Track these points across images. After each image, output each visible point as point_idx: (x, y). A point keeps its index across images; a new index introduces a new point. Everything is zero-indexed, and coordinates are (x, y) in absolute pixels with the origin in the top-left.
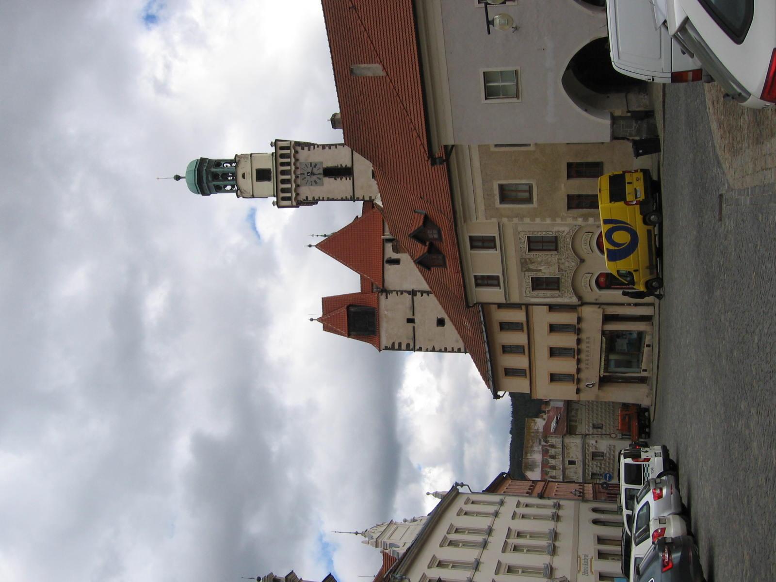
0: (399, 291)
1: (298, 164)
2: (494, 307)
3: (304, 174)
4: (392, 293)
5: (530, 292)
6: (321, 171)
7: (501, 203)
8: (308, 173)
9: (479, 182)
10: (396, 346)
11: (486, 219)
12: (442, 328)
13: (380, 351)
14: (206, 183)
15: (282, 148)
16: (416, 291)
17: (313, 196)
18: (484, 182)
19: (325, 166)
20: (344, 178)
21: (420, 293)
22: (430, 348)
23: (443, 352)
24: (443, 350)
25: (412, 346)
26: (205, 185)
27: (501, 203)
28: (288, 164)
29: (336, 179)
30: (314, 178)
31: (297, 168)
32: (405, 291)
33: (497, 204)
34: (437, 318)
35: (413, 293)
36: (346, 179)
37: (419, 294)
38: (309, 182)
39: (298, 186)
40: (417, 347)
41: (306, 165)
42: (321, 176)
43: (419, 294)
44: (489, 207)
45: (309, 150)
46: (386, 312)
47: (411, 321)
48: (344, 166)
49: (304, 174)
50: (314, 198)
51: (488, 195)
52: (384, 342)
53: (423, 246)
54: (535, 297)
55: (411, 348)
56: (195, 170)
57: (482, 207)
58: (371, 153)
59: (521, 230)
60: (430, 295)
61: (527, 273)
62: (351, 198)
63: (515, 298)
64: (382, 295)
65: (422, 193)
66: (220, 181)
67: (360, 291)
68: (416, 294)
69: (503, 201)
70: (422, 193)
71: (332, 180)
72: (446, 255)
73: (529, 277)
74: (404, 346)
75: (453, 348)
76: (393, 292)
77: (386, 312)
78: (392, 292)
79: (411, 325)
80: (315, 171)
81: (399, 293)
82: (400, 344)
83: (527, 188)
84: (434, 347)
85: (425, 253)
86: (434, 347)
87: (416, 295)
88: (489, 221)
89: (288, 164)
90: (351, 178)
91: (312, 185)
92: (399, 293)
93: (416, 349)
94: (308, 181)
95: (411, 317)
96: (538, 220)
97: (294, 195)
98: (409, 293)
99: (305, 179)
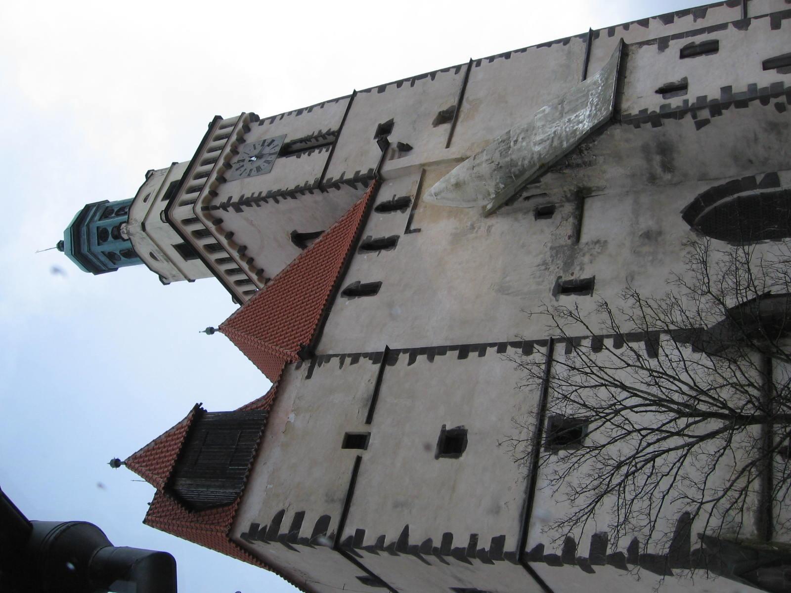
0: (349, 355)
1: (241, 149)
3: (243, 161)
4: (328, 361)
6: (278, 149)
12: (453, 460)
14: (88, 225)
16: (398, 352)
19: (287, 140)
20: (317, 151)
21: (407, 355)
22: (392, 537)
24: (437, 543)
25: (333, 527)
26: (84, 229)
30: (261, 163)
31: (235, 151)
32: (366, 355)
34: (444, 426)
35: (387, 358)
36: (320, 152)
37: (404, 358)
38: (248, 171)
39: (222, 180)
41: (254, 145)
43: (404, 358)
46: (292, 416)
48: (324, 131)
49: (243, 161)
52: (256, 509)
60: (437, 358)
64: (298, 368)
68: (396, 360)
71: (293, 159)
75: (474, 538)
77: (292, 416)
79: (354, 452)
81: (348, 360)
82: (299, 517)
84: (407, 528)
86: (407, 528)
91: (249, 175)
92: (348, 360)
93: (344, 537)
94: (245, 169)
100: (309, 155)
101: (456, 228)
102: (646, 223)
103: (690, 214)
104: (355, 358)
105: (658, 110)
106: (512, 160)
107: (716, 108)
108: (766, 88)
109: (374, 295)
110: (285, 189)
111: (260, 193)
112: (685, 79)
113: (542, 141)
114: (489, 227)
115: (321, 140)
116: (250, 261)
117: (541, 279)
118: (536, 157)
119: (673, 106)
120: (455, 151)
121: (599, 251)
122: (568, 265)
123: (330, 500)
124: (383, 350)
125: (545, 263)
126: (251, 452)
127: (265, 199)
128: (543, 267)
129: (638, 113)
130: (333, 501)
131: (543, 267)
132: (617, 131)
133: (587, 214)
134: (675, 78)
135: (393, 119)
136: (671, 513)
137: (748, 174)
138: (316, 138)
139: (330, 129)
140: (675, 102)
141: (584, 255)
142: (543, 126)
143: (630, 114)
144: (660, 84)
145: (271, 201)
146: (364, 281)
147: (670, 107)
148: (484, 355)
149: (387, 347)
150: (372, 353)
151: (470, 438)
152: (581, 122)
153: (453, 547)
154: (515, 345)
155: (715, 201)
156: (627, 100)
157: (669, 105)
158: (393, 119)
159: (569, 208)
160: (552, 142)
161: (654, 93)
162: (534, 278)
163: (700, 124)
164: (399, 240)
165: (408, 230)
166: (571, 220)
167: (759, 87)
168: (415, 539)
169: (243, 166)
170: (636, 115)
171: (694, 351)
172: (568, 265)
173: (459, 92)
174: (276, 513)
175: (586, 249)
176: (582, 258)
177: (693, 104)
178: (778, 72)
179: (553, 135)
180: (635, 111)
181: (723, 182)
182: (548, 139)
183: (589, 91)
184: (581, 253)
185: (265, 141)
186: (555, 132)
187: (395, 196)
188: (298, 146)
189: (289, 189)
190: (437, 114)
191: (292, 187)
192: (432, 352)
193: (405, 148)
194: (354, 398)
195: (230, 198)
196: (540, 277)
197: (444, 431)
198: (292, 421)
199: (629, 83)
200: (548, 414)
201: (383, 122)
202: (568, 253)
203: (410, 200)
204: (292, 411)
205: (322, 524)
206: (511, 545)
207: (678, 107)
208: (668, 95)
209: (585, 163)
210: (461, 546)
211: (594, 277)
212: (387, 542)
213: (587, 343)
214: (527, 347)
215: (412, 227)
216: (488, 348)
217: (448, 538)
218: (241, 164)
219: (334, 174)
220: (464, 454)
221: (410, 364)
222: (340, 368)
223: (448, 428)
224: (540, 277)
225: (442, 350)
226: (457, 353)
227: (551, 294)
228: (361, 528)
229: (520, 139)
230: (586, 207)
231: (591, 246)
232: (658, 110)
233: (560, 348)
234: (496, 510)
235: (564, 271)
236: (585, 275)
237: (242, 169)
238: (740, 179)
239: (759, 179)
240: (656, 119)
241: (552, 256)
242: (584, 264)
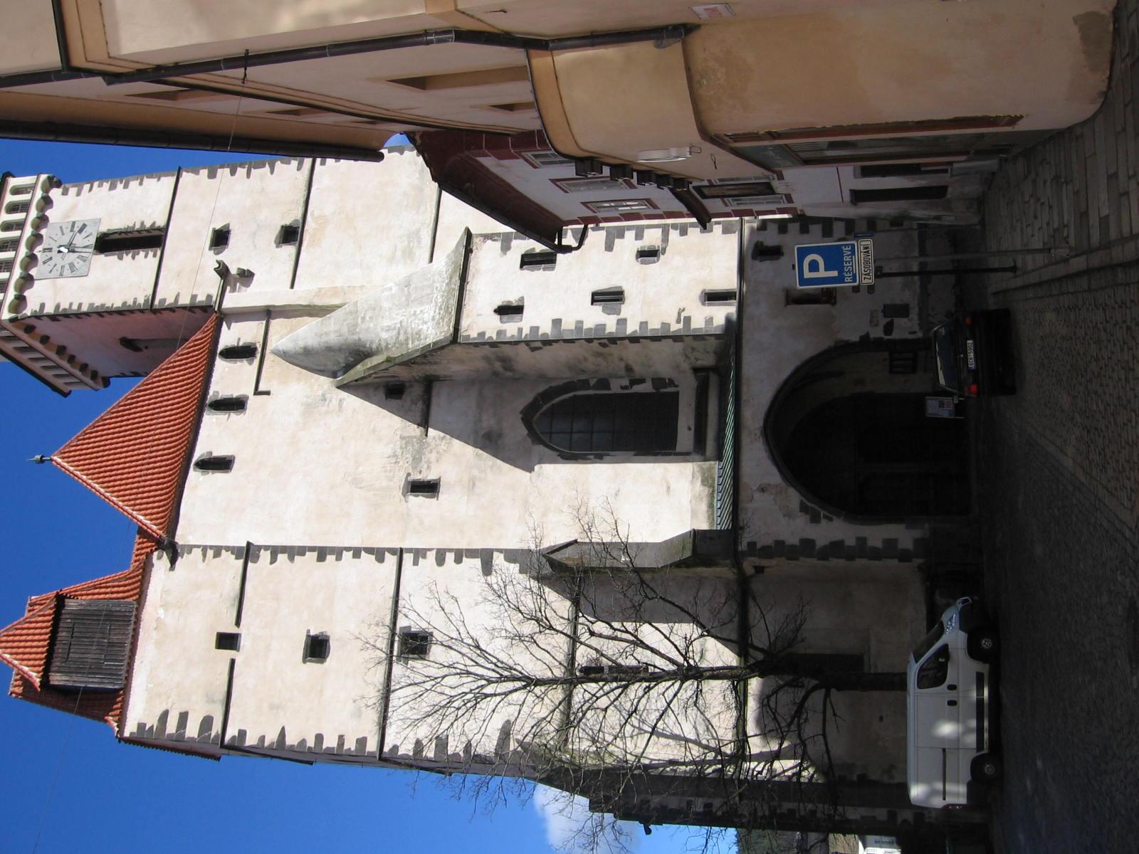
0: (211, 547)
3: (50, 250)
4: (190, 552)
6: (92, 241)
8: (61, 246)
16: (259, 548)
17: (57, 302)
19: (104, 229)
20: (142, 253)
24: (311, 743)
25: (217, 728)
29: (121, 258)
31: (37, 238)
32: (228, 549)
34: (308, 631)
35: (248, 553)
36: (146, 256)
37: (265, 556)
38: (59, 267)
41: (61, 227)
43: (265, 556)
46: (161, 612)
47: (227, 641)
48: (148, 225)
49: (50, 250)
55: (213, 733)
60: (297, 558)
62: (146, 301)
64: (160, 558)
68: (258, 557)
75: (341, 738)
76: (194, 550)
78: (190, 548)
79: (229, 654)
80: (80, 241)
81: (210, 553)
82: (184, 717)
84: (283, 729)
86: (283, 729)
90: (159, 253)
91: (61, 275)
92: (210, 553)
93: (228, 738)
95: (232, 629)
99: (49, 263)
100: (133, 258)
101: (307, 397)
102: (488, 422)
103: (528, 416)
104: (218, 551)
105: (495, 337)
106: (360, 339)
107: (547, 342)
108: (590, 329)
109: (227, 472)
110: (110, 305)
111: (80, 305)
112: (522, 299)
113: (388, 329)
114: (340, 401)
115: (145, 234)
116: (72, 359)
117: (392, 474)
118: (383, 344)
119: (509, 334)
120: (299, 296)
121: (445, 448)
122: (417, 460)
123: (210, 700)
124: (244, 545)
125: (395, 455)
126: (125, 647)
127: (87, 314)
128: (394, 460)
129: (475, 335)
130: (213, 701)
131: (393, 460)
132: (458, 349)
133: (434, 401)
134: (513, 299)
135: (229, 224)
136: (497, 723)
137: (583, 377)
138: (139, 231)
139: (154, 223)
140: (511, 328)
141: (431, 451)
142: (390, 309)
143: (469, 336)
144: (498, 302)
145: (95, 316)
146: (217, 453)
147: (505, 335)
148: (341, 560)
149: (249, 544)
150: (234, 547)
151: (333, 645)
152: (426, 323)
153: (324, 747)
154: (370, 551)
155: (552, 399)
156: (468, 316)
157: (505, 331)
158: (229, 224)
159: (417, 391)
160: (399, 334)
161: (493, 313)
162: (385, 471)
163: (533, 349)
164: (249, 402)
165: (257, 392)
166: (420, 404)
167: (586, 326)
168: (291, 740)
169: (51, 259)
170: (475, 339)
171: (521, 572)
172: (417, 460)
173: (303, 200)
174: (161, 712)
175: (433, 445)
176: (429, 455)
177: (526, 335)
178: (603, 311)
179: (399, 325)
180: (474, 334)
181: (561, 383)
182: (394, 329)
183: (434, 282)
184: (429, 449)
185: (74, 223)
186: (401, 322)
187: (239, 339)
188: (116, 236)
189: (115, 306)
190: (279, 228)
191: (118, 304)
192: (294, 552)
193: (246, 276)
194: (221, 596)
195: (43, 306)
196: (390, 471)
197: (308, 636)
198: (162, 617)
199: (470, 291)
200: (398, 627)
201: (218, 227)
202: (417, 446)
203: (256, 349)
204: (161, 606)
205: (207, 722)
206: (372, 746)
207: (513, 336)
208: (505, 317)
209: (430, 362)
210: (331, 745)
211: (440, 479)
212: (267, 744)
213: (431, 556)
214: (379, 554)
215: (261, 388)
216: (344, 552)
218: (49, 254)
219: (167, 294)
220: (328, 659)
221: (272, 563)
222: (204, 561)
223: (312, 633)
224: (390, 471)
225: (302, 551)
226: (315, 554)
227: (400, 493)
228: (243, 728)
229: (367, 318)
230: (434, 392)
231: (438, 442)
232: (495, 337)
233: (408, 558)
234: (358, 714)
235: (413, 468)
236: (430, 476)
237: (52, 263)
238: (575, 380)
239: (592, 382)
240: (493, 345)
241: (401, 448)
242: (431, 463)
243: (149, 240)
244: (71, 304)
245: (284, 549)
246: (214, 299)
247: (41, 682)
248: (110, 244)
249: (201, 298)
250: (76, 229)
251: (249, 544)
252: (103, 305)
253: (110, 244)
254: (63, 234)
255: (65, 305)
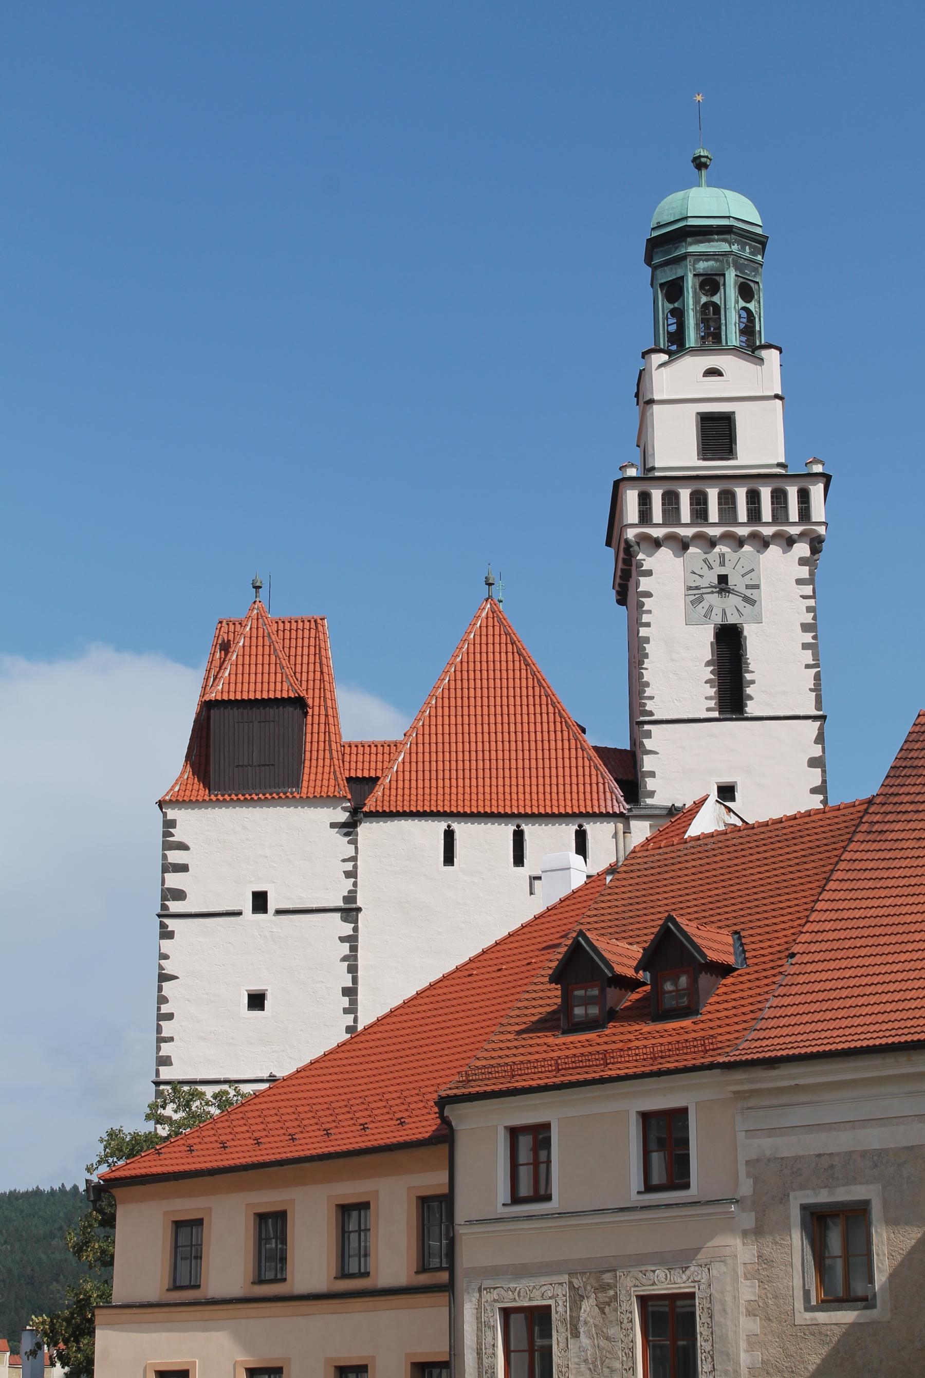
0: (355, 867)
2: (433, 1181)
3: (722, 564)
4: (349, 842)
5: (495, 1301)
6: (731, 620)
7: (804, 1207)
9: (874, 1139)
10: (175, 857)
11: (747, 1162)
13: (161, 804)
15: (804, 496)
16: (356, 922)
18: (877, 1157)
19: (749, 631)
20: (712, 692)
22: (169, 967)
23: (159, 1009)
24: (165, 1009)
25: (175, 906)
27: (804, 1207)
28: (754, 515)
31: (740, 542)
32: (355, 884)
33: (799, 1199)
35: (349, 911)
40: (172, 924)
42: (719, 620)
44: (793, 1171)
45: (799, 582)
47: (260, 901)
49: (722, 564)
50: (648, 595)
51: (829, 1168)
53: (635, 963)
54: (478, 1319)
56: (729, 217)
57: (789, 1147)
58: (906, 799)
59: (714, 1272)
61: (566, 1287)
63: (471, 1253)
64: (345, 809)
65: (806, 958)
66: (696, 301)
67: (345, 739)
69: (812, 1214)
70: (806, 958)
71: (707, 654)
72: (607, 1031)
73: (550, 1298)
74: (174, 880)
78: (354, 842)
79: (247, 905)
81: (349, 866)
82: (184, 868)
83: (859, 1288)
84: (177, 978)
85: (611, 968)
86: (177, 978)
87: (345, 920)
88: (742, 1170)
89: (754, 515)
93: (167, 921)
95: (272, 905)
96: (748, 1325)
97: (658, 533)
98: (351, 898)
104: (351, 874)
149: (359, 910)
205: (179, 895)
217: (170, 1017)
218: (715, 565)
225: (353, 969)
226: (350, 984)
243: (731, 698)
244: (649, 612)
245: (354, 949)
246: (649, 801)
247: (211, 700)
248: (729, 644)
249: (650, 784)
250: (748, 593)
251: (359, 910)
252: (646, 656)
253: (729, 644)
254: (743, 576)
255: (648, 603)
